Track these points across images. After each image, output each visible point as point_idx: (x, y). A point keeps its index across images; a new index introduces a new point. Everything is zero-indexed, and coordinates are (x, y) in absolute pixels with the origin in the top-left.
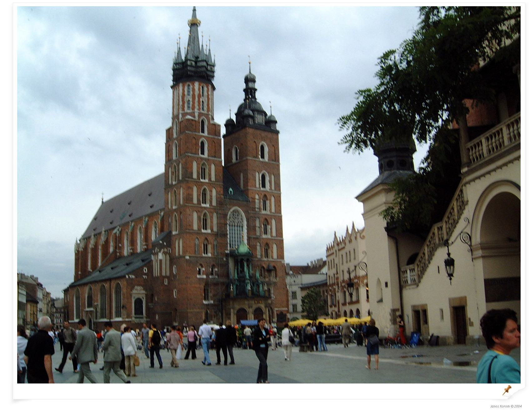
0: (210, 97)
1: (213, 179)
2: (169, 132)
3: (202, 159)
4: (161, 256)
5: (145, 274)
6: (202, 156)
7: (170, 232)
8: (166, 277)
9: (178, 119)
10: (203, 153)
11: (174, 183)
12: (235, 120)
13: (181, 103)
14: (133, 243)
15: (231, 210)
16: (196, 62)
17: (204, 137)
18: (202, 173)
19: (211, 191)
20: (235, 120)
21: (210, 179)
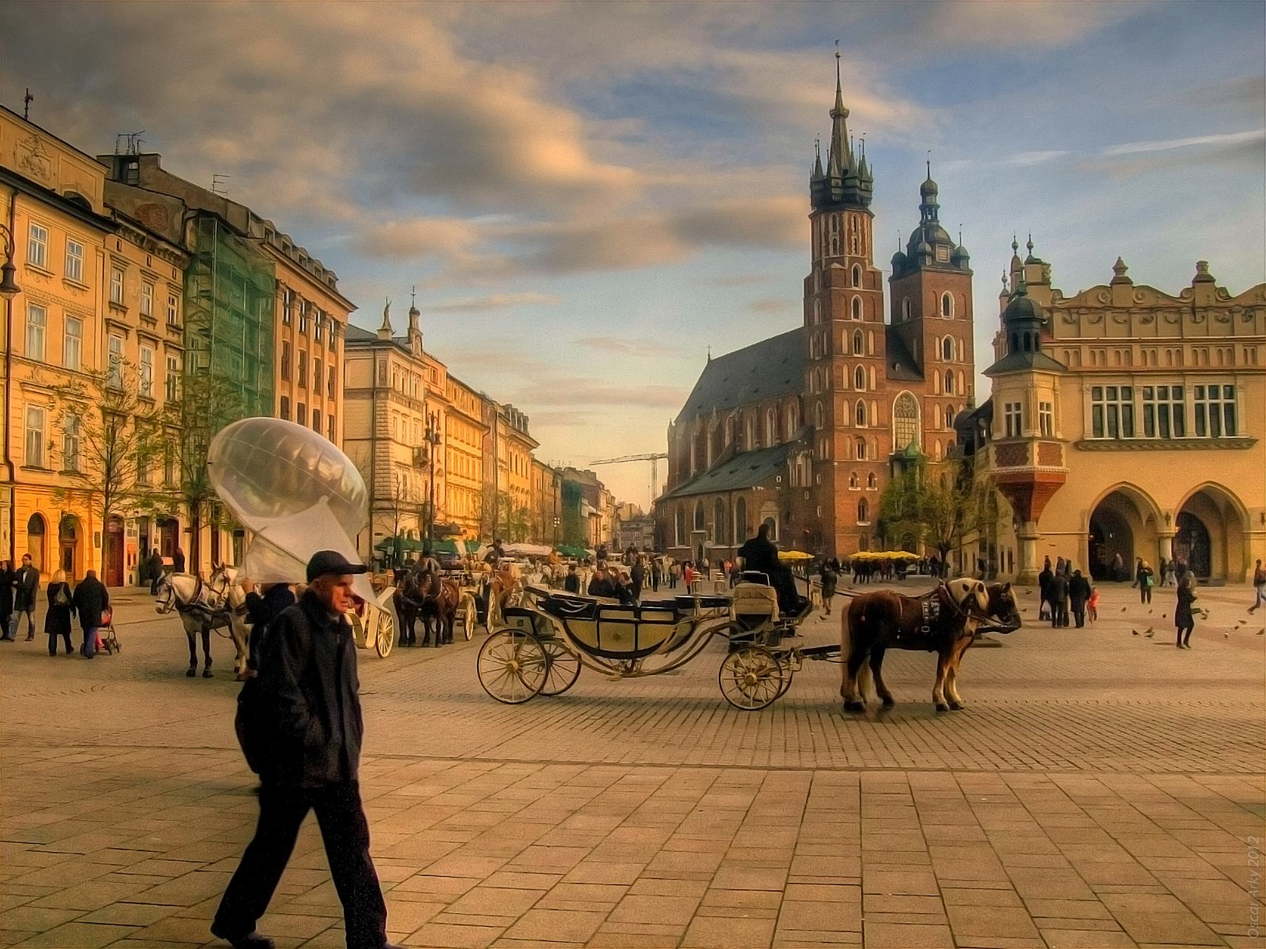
0: (866, 232)
1: (871, 352)
2: (808, 282)
3: (855, 325)
4: (800, 460)
5: (779, 484)
6: (856, 320)
7: (813, 428)
8: (806, 489)
9: (821, 268)
10: (856, 316)
11: (817, 358)
12: (906, 255)
13: (824, 245)
14: (760, 433)
15: (900, 394)
16: (844, 181)
17: (856, 292)
18: (857, 343)
19: (869, 370)
20: (906, 255)
21: (867, 351)
